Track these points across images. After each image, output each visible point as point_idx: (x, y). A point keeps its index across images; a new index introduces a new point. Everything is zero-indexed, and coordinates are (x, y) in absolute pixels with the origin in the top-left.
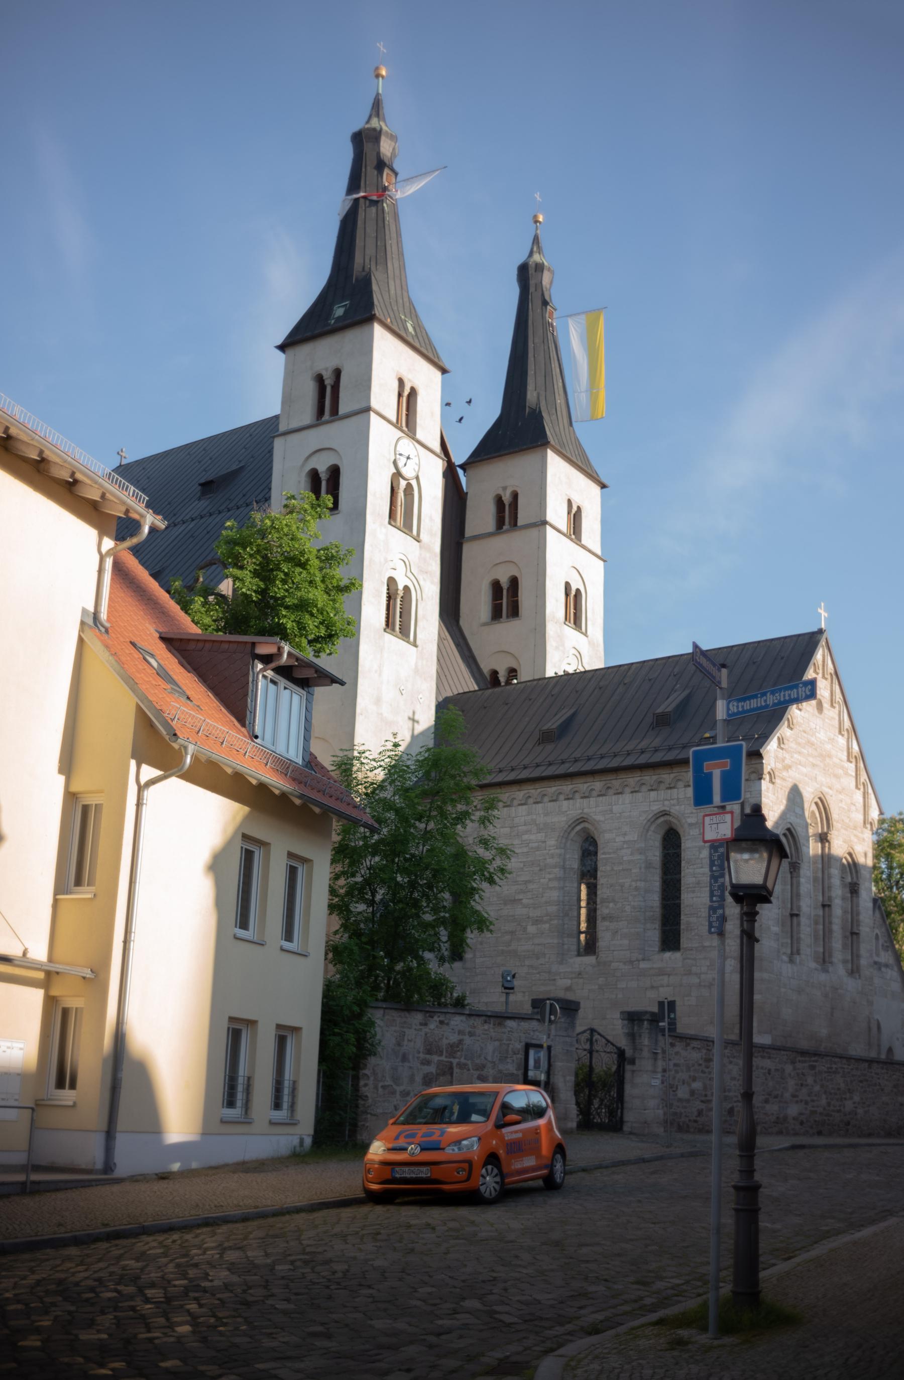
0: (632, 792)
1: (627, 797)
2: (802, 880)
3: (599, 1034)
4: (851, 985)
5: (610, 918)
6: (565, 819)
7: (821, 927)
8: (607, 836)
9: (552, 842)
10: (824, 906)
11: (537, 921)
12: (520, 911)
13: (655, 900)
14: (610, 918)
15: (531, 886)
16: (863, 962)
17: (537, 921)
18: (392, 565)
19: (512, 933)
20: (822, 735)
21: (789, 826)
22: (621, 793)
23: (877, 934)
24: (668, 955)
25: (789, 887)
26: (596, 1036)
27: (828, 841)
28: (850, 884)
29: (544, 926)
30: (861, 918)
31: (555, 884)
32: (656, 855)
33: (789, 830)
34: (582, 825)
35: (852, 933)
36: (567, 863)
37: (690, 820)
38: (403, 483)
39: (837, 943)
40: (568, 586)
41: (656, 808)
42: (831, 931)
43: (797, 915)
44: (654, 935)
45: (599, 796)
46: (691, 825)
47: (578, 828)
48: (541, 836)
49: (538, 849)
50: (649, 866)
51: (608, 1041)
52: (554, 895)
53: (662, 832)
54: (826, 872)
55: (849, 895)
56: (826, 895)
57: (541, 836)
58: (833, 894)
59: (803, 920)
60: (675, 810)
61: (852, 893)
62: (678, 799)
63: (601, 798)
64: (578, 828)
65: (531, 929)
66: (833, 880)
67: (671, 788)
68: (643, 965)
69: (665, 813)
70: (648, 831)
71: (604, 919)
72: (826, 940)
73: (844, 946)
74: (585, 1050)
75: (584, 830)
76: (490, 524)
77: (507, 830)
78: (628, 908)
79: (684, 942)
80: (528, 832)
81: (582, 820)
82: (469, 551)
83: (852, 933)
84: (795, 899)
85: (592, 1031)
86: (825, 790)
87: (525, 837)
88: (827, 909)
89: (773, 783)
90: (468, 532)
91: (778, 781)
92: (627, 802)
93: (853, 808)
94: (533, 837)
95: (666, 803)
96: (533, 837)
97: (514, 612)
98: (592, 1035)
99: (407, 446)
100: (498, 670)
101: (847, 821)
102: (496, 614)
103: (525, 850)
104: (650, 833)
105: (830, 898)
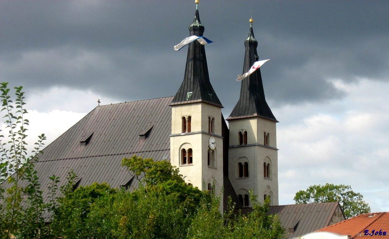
38: (211, 151)
40: (265, 163)
82: (231, 152)
97: (247, 175)
100: (242, 194)
102: (241, 175)
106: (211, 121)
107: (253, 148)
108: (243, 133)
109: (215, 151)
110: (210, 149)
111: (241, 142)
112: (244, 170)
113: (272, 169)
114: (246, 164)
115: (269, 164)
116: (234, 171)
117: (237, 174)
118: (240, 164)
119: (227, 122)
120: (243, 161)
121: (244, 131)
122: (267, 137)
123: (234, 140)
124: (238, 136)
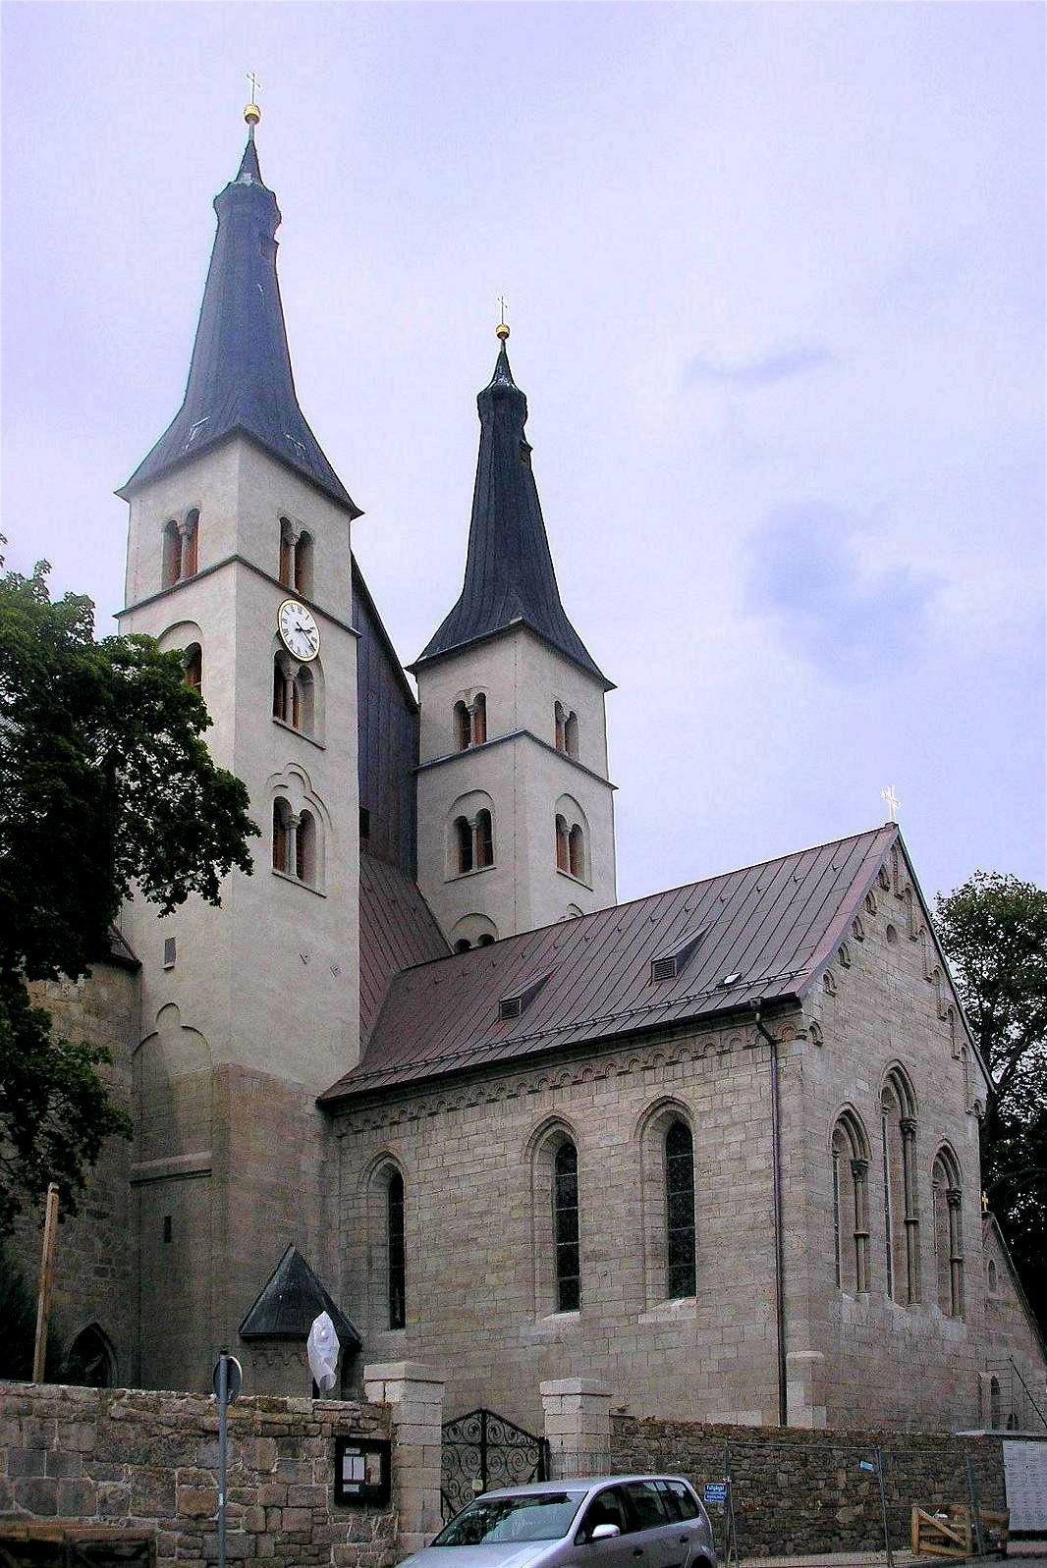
0: (620, 1074)
1: (613, 1082)
2: (872, 1186)
3: (499, 1418)
4: (954, 1332)
5: (596, 1256)
6: (529, 1120)
7: (905, 1253)
8: (588, 1140)
9: (514, 1155)
10: (907, 1223)
11: (499, 1268)
12: (477, 1255)
13: (657, 1227)
14: (596, 1256)
15: (488, 1220)
16: (968, 1300)
17: (499, 1268)
18: (279, 780)
19: (467, 1286)
20: (896, 979)
21: (847, 1107)
22: (604, 1077)
23: (991, 1261)
24: (678, 1302)
25: (853, 1197)
26: (492, 1423)
27: (913, 1133)
28: (948, 1191)
29: (509, 1273)
30: (965, 1239)
31: (518, 1213)
32: (655, 1161)
33: (847, 1113)
34: (554, 1129)
35: (953, 1261)
36: (536, 1183)
37: (701, 1108)
39: (929, 1276)
40: (560, 820)
41: (654, 1093)
42: (918, 1258)
43: (865, 1237)
44: (658, 1274)
45: (574, 1083)
46: (702, 1114)
47: (549, 1132)
48: (498, 1149)
49: (496, 1166)
50: (647, 1179)
51: (516, 1428)
52: (520, 1229)
53: (666, 1128)
54: (910, 1174)
55: (947, 1207)
56: (911, 1206)
57: (498, 1149)
58: (921, 1206)
59: (876, 1244)
60: (679, 1095)
61: (950, 1205)
62: (684, 1077)
63: (577, 1087)
64: (549, 1132)
65: (491, 1279)
66: (920, 1186)
67: (674, 1063)
68: (643, 1320)
69: (667, 1101)
70: (644, 1129)
71: (587, 1259)
72: (913, 1270)
73: (941, 1278)
74: (471, 1444)
75: (559, 1134)
76: (450, 745)
77: (455, 1143)
78: (619, 1241)
79: (699, 1288)
80: (483, 1143)
81: (554, 1120)
83: (953, 1261)
84: (861, 1215)
85: (484, 1413)
86: (904, 1057)
87: (479, 1150)
88: (912, 1227)
89: (819, 1044)
90: (425, 758)
91: (827, 1042)
92: (613, 1088)
93: (949, 1084)
94: (488, 1150)
95: (668, 1085)
96: (488, 1150)
97: (488, 858)
98: (484, 1418)
99: (294, 615)
100: (467, 937)
101: (939, 1101)
102: (466, 864)
103: (479, 1169)
104: (647, 1131)
105: (916, 1212)
106: (295, 541)
107: (509, 748)
108: (470, 702)
109: (313, 668)
110: (283, 656)
111: (465, 737)
112: (475, 842)
113: (590, 846)
114: (485, 817)
115: (576, 827)
116: (438, 847)
117: (450, 865)
118: (462, 825)
119: (410, 677)
120: (470, 811)
121: (473, 696)
122: (566, 724)
123: (439, 731)
124: (448, 721)
